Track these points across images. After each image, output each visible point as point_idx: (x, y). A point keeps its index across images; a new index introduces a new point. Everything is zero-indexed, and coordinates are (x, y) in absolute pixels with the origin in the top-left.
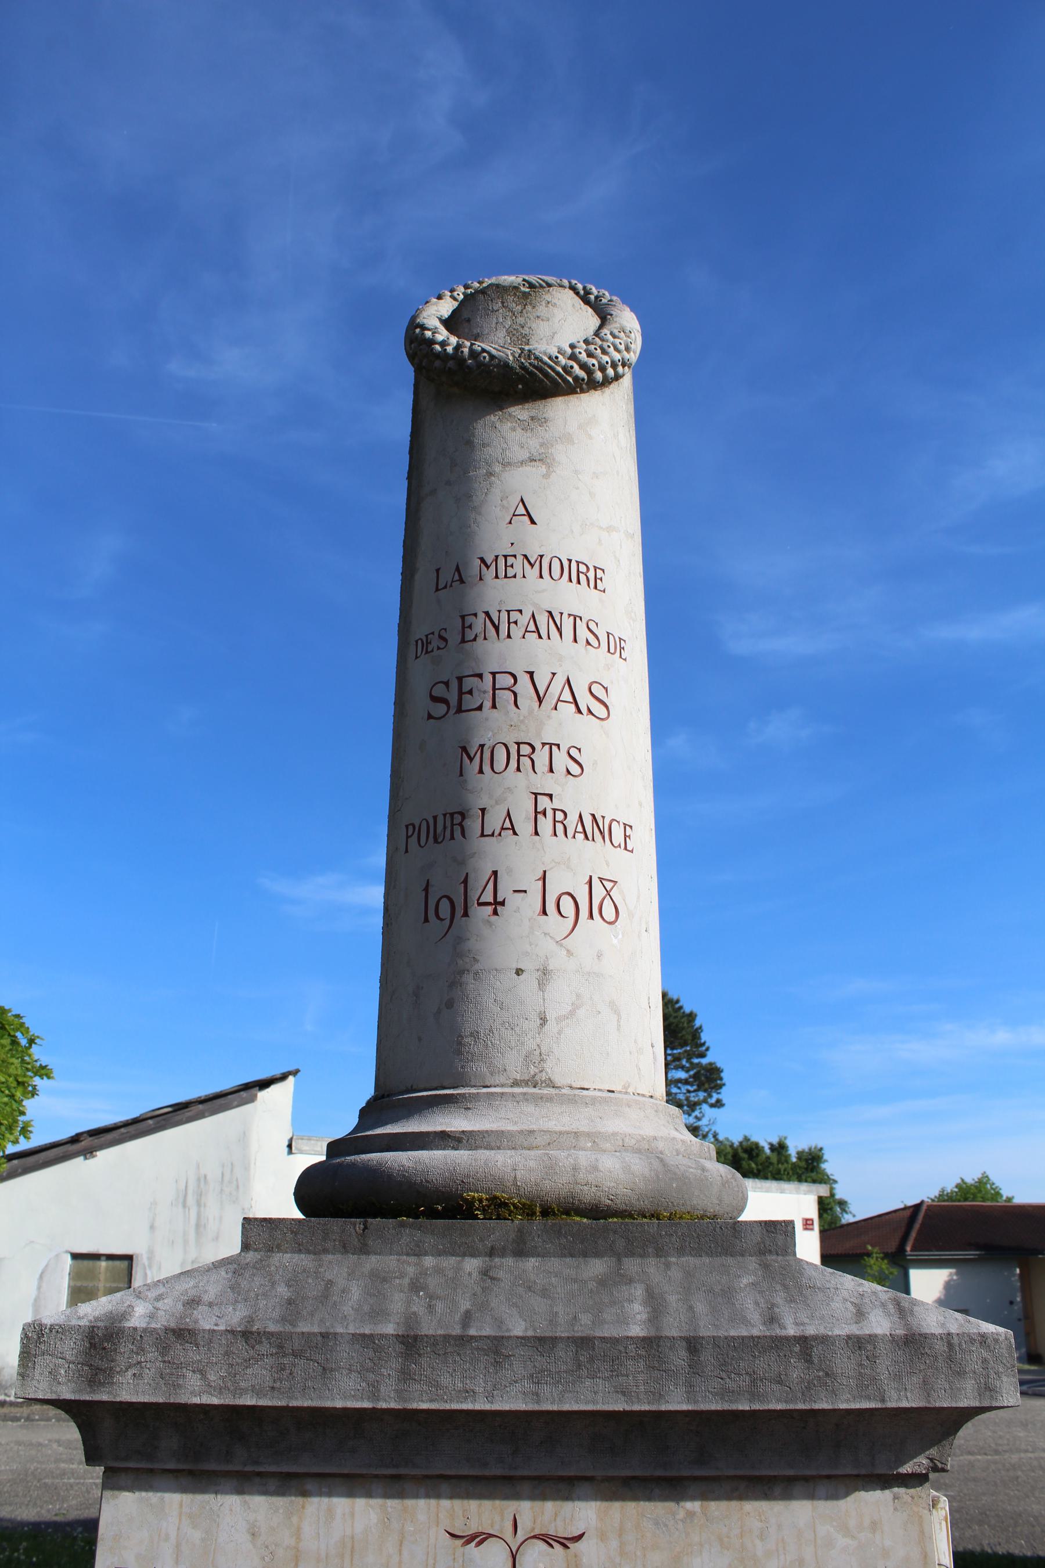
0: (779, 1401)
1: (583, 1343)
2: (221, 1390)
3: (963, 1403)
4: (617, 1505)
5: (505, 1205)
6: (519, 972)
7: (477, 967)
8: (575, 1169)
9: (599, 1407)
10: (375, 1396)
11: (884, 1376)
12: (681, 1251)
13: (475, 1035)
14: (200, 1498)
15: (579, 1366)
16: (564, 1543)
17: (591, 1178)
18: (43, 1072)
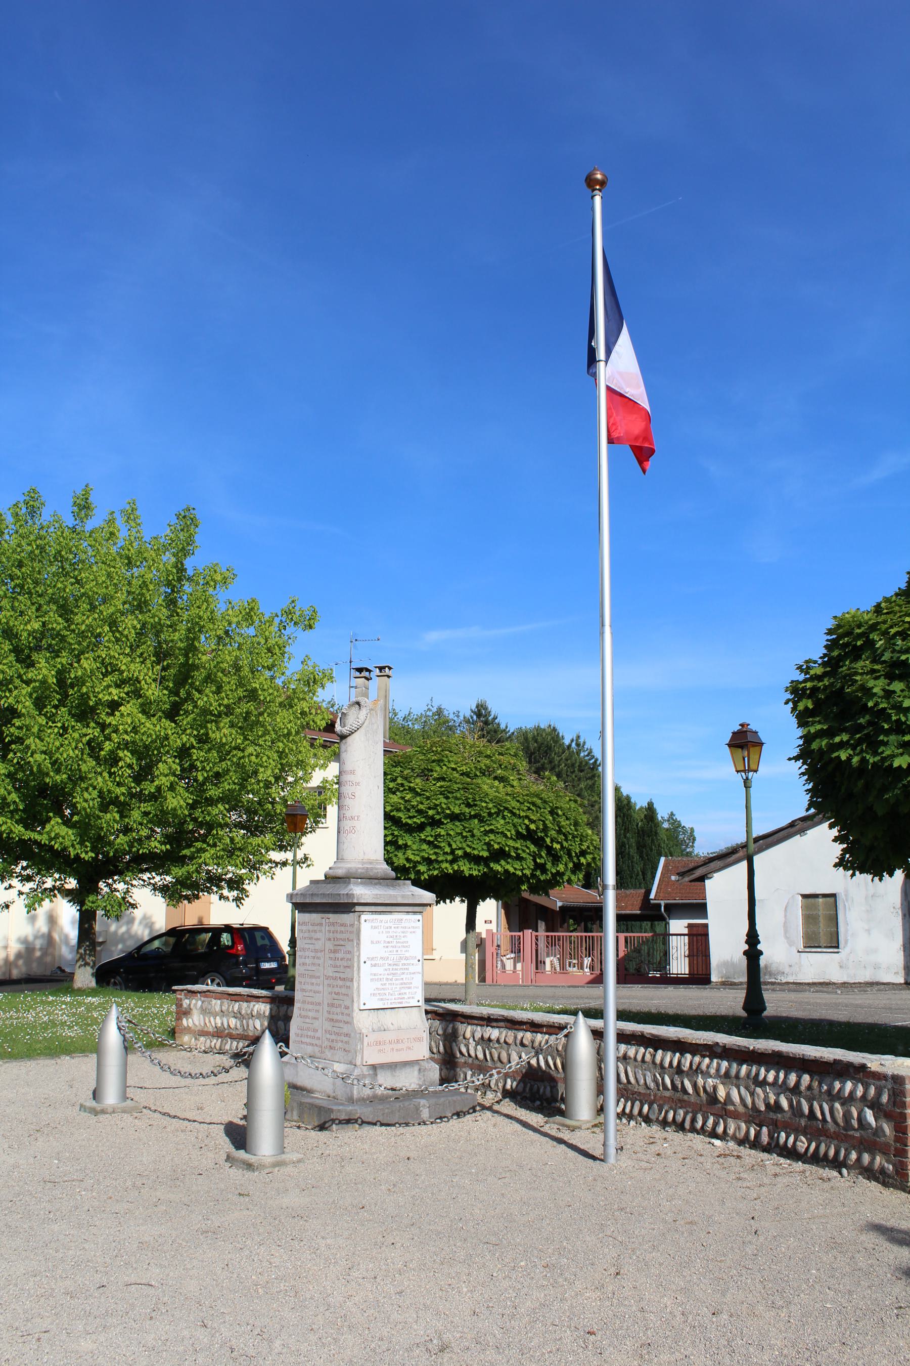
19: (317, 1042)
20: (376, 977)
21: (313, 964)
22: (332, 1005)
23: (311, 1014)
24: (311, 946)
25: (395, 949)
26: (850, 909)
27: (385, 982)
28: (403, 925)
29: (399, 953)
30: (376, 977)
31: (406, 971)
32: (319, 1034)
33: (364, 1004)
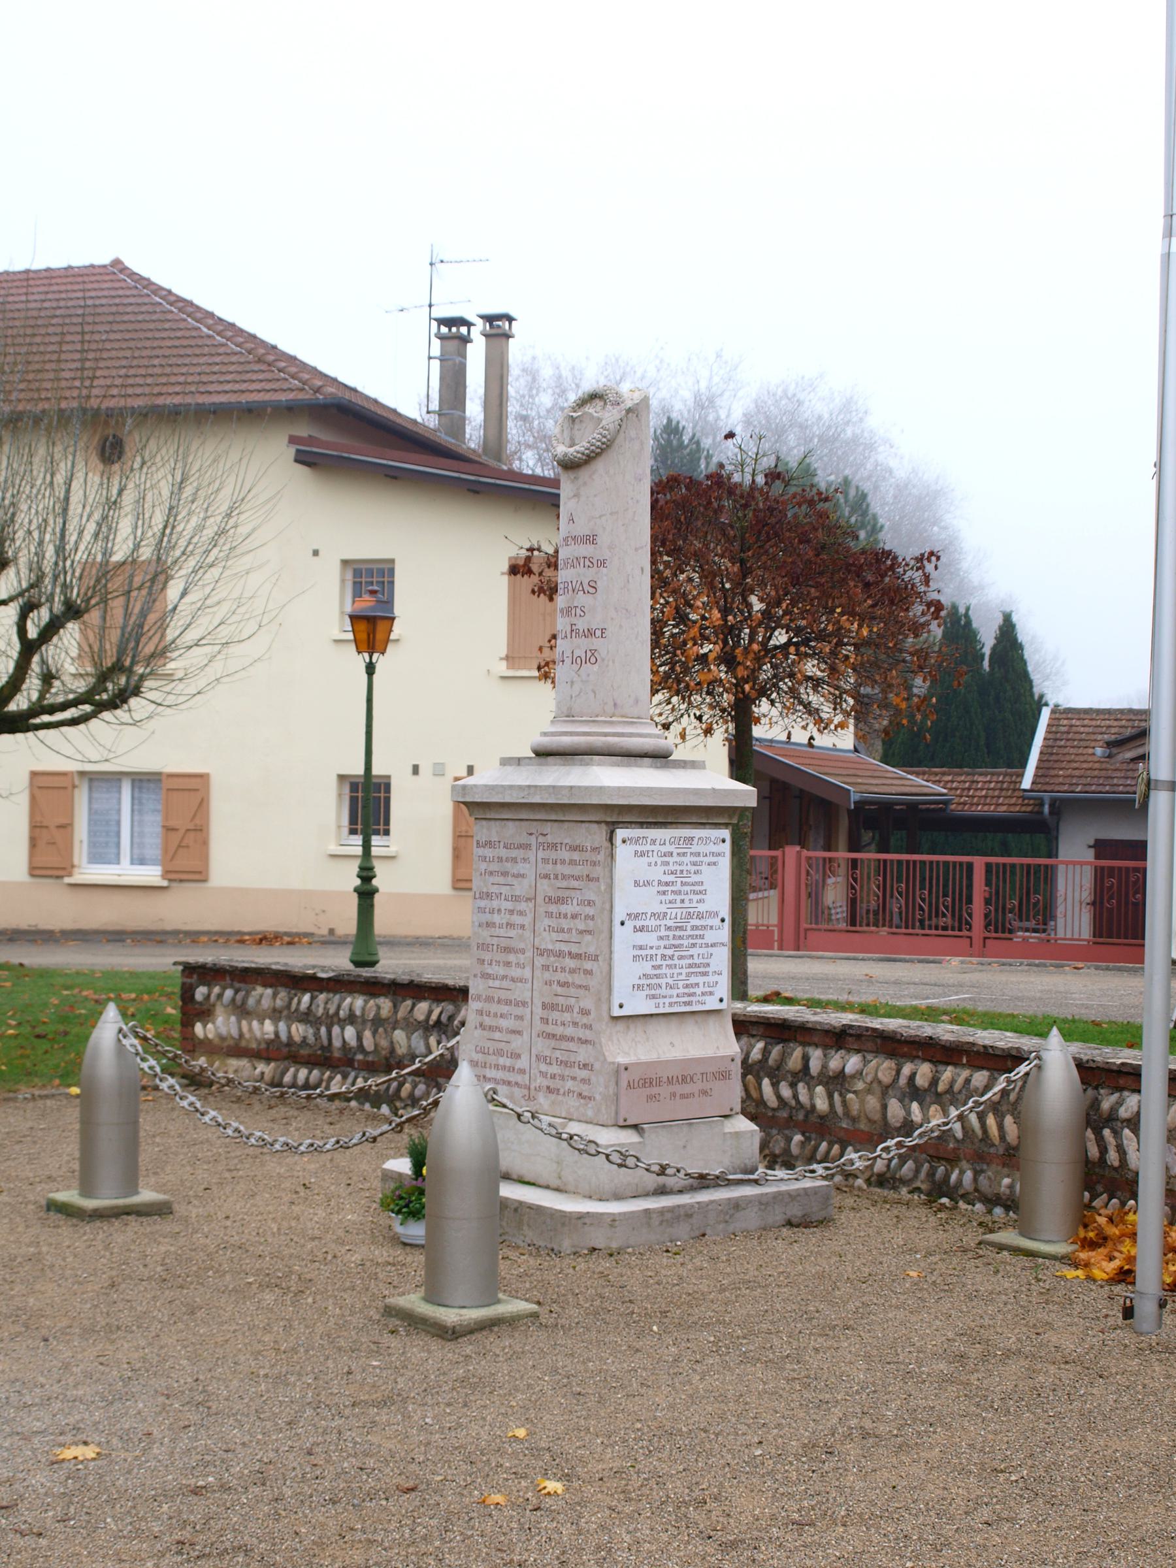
19: (519, 1078)
20: (643, 953)
21: (510, 925)
22: (553, 1007)
23: (504, 1023)
24: (505, 890)
25: (679, 898)
27: (659, 962)
28: (695, 848)
29: (687, 904)
30: (643, 953)
31: (699, 941)
32: (523, 1063)
33: (621, 1006)
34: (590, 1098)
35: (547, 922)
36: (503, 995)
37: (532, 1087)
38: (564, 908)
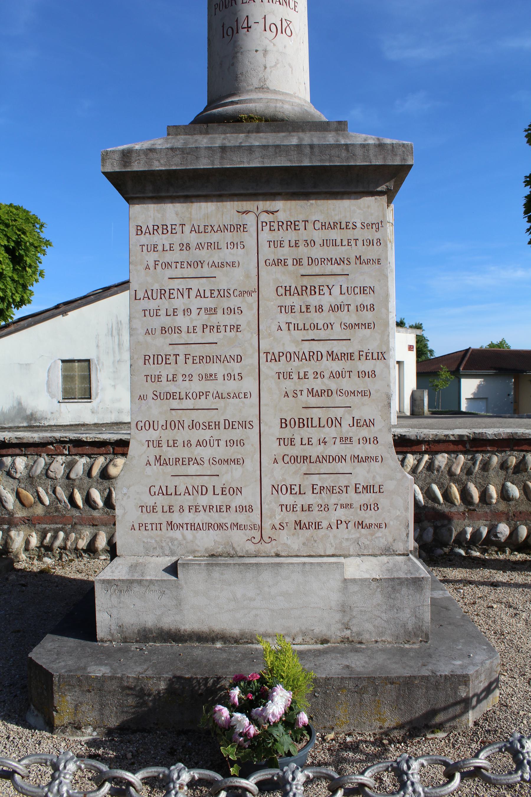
0: (338, 162)
1: (277, 146)
2: (165, 166)
3: (396, 163)
4: (289, 202)
5: (253, 118)
6: (256, 51)
7: (242, 50)
8: (276, 107)
9: (282, 165)
10: (213, 164)
11: (371, 156)
12: (310, 131)
13: (242, 74)
14: (160, 205)
15: (276, 153)
16: (272, 213)
17: (281, 110)
18: (48, 243)
19: (241, 518)
22: (301, 423)
23: (205, 453)
24: (194, 284)
26: (100, 371)
34: (379, 526)
35: (283, 318)
36: (201, 417)
37: (267, 526)
38: (314, 300)
